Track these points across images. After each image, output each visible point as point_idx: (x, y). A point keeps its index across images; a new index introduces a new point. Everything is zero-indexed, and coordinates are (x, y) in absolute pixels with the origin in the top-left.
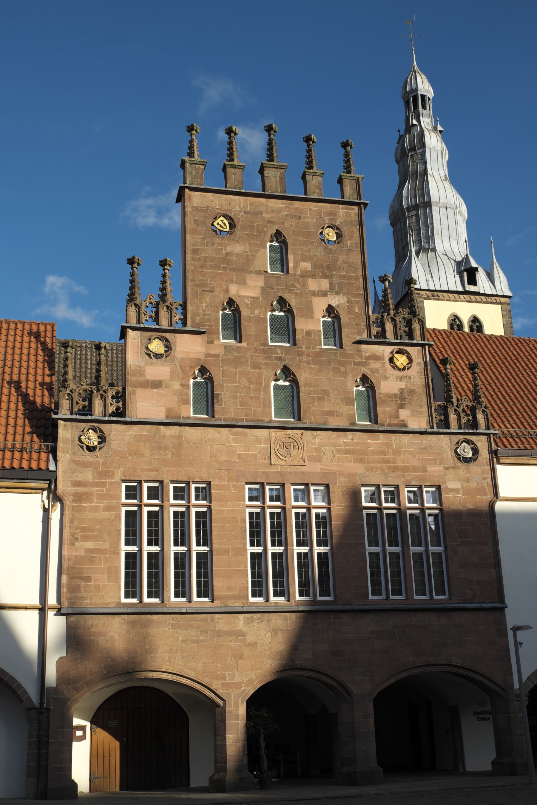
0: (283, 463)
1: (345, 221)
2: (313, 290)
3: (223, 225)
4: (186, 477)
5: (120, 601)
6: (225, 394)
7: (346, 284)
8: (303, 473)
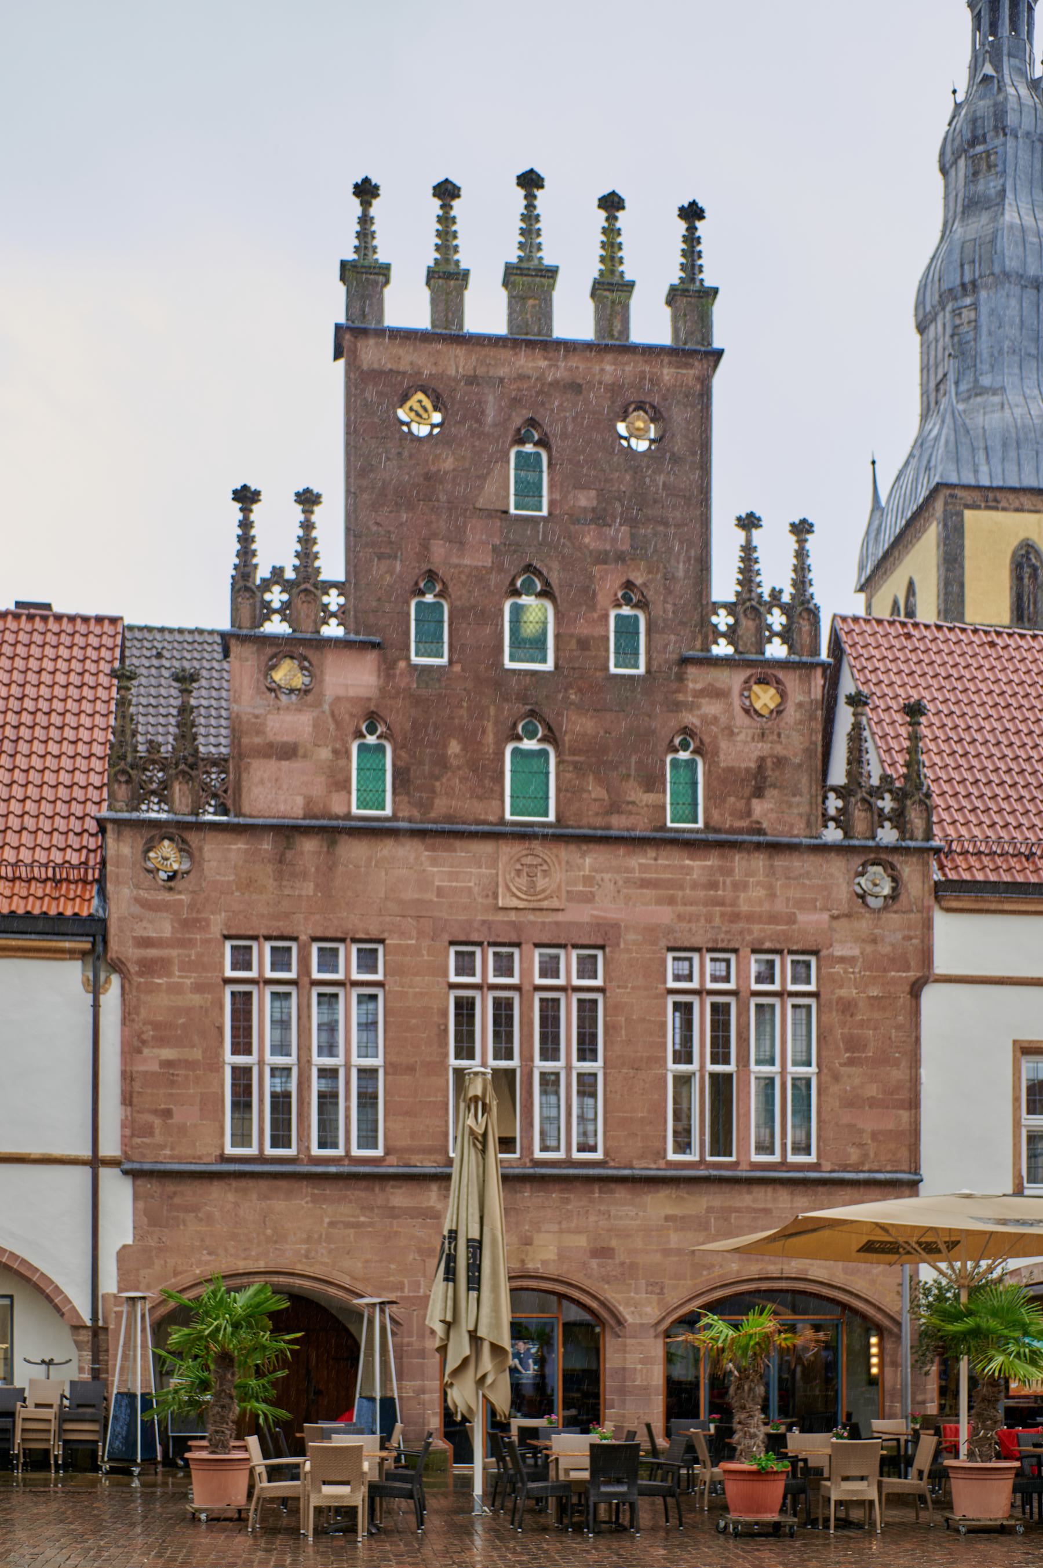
0: (521, 905)
8: (557, 924)
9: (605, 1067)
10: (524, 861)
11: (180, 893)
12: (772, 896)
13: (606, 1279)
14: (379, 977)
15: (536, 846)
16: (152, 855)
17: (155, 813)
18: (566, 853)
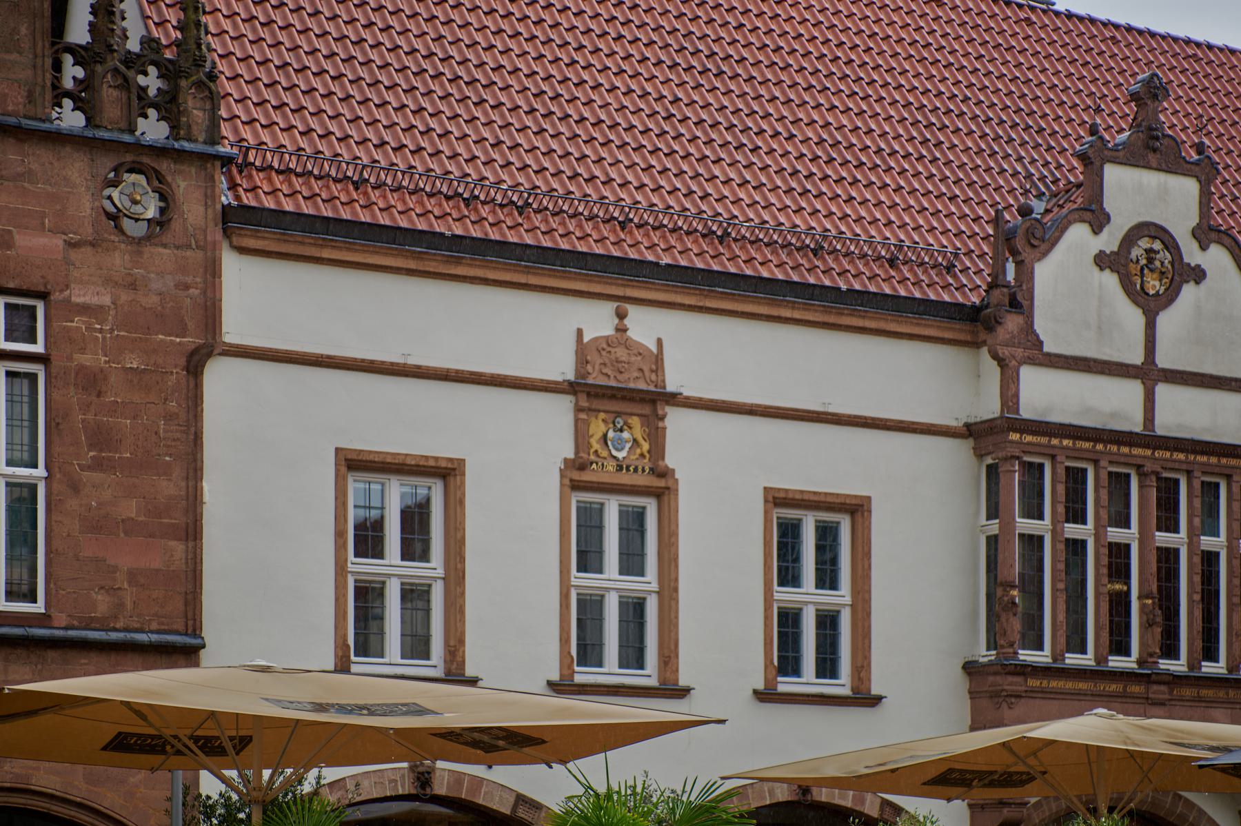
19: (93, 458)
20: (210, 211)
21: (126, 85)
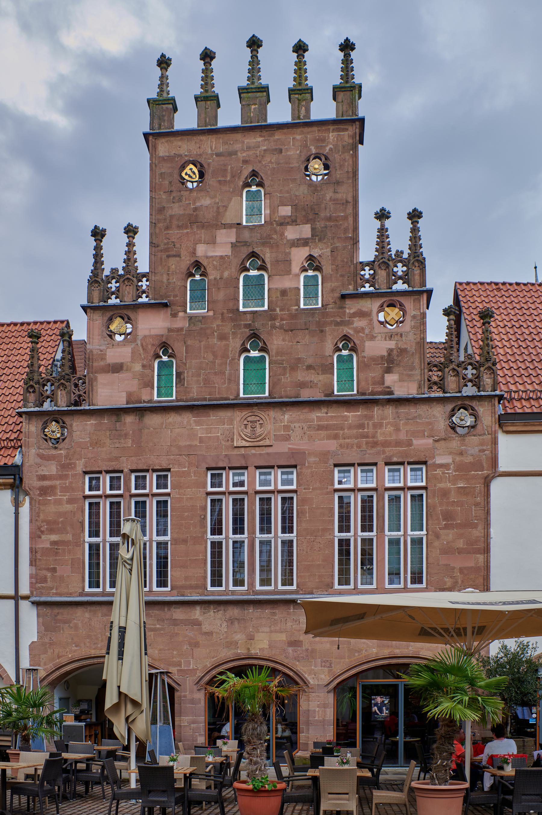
0: (247, 444)
1: (336, 146)
2: (292, 240)
3: (191, 174)
4: (146, 465)
5: (84, 590)
6: (188, 372)
7: (331, 227)
8: (268, 454)
9: (297, 536)
10: (249, 419)
11: (61, 450)
12: (398, 430)
13: (297, 659)
14: (168, 491)
15: (255, 409)
16: (46, 430)
17: (47, 406)
18: (273, 413)
19: (445, 524)
20: (493, 419)
21: (457, 374)
